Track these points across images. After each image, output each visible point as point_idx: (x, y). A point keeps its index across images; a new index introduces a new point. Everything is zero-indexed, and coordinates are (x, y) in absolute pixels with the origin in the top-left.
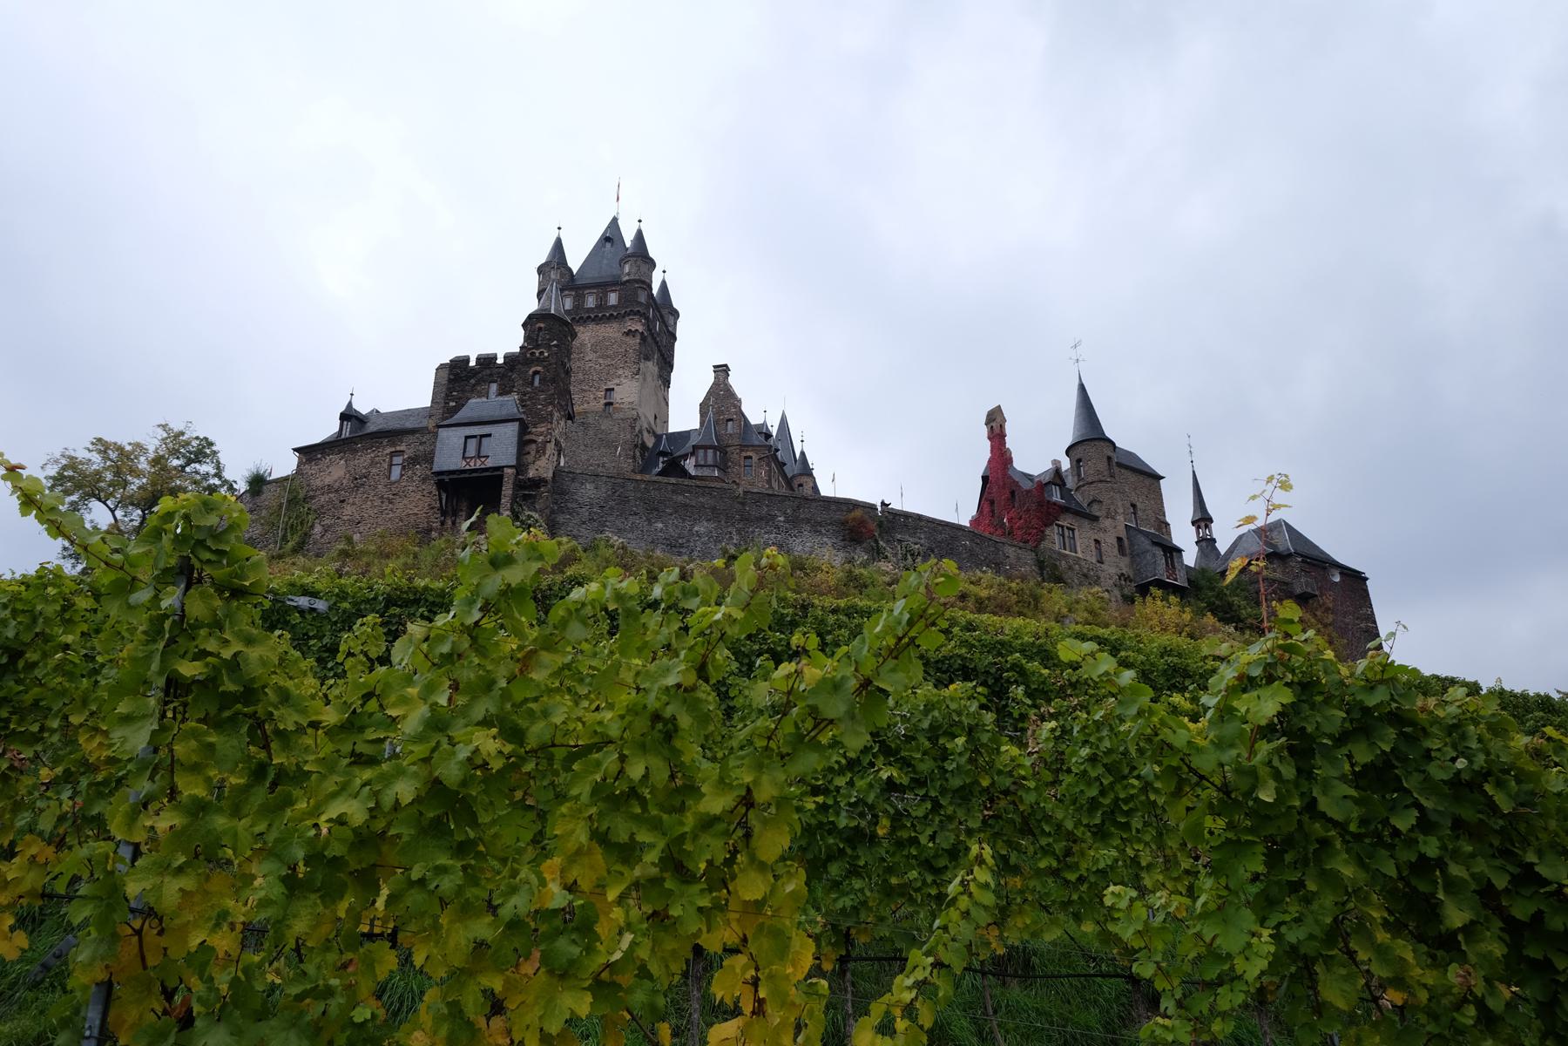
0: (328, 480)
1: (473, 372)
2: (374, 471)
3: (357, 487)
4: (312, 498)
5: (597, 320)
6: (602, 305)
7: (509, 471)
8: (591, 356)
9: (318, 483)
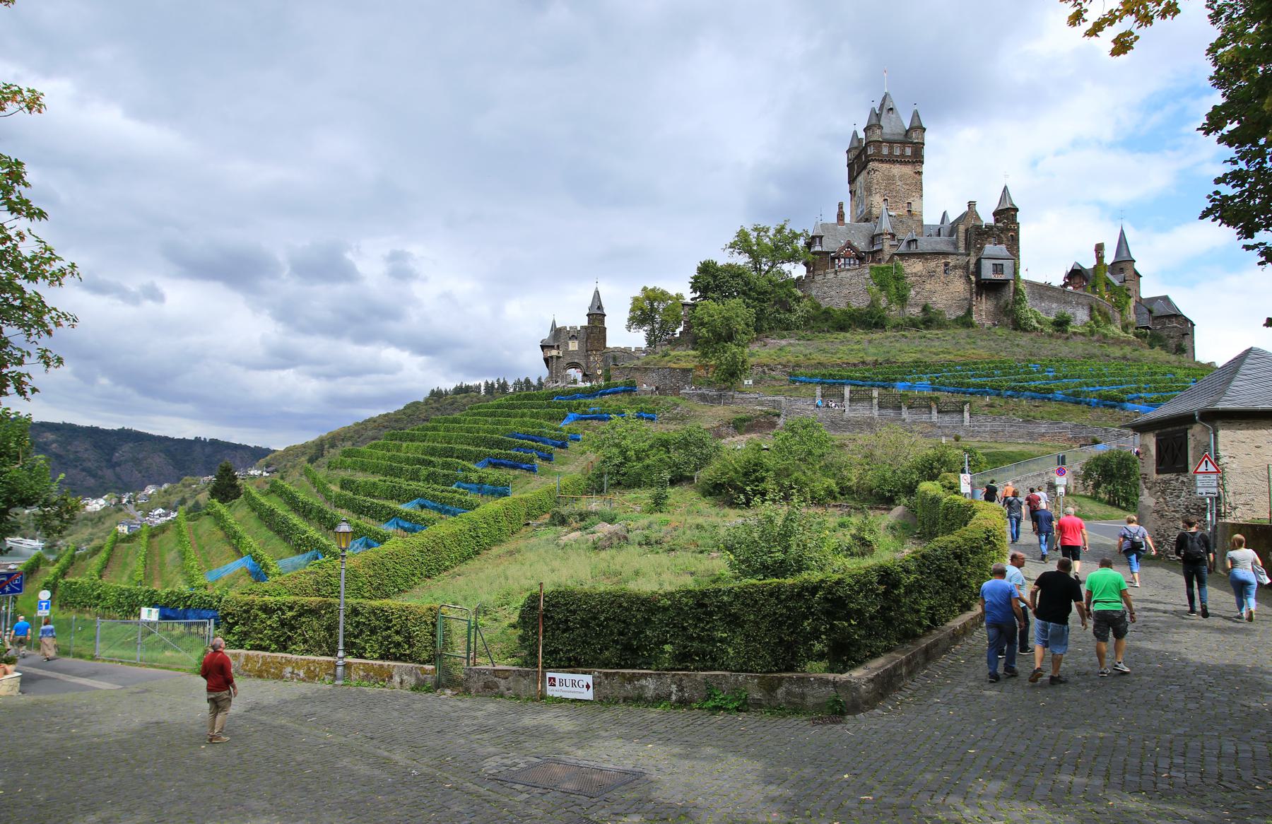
0: (914, 271)
1: (986, 233)
2: (938, 270)
3: (932, 276)
4: (907, 277)
5: (901, 163)
6: (903, 155)
7: (1012, 282)
8: (899, 183)
9: (908, 271)
